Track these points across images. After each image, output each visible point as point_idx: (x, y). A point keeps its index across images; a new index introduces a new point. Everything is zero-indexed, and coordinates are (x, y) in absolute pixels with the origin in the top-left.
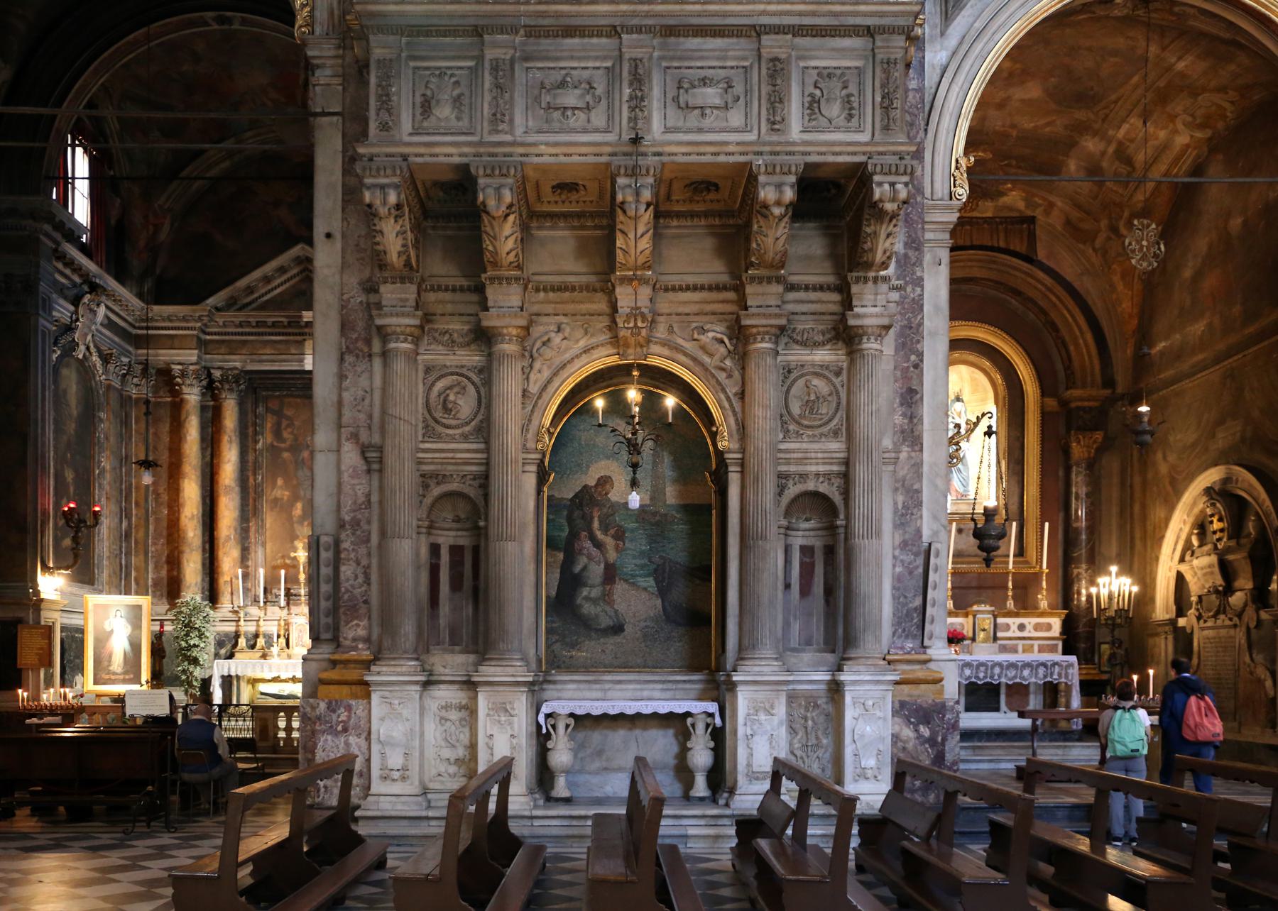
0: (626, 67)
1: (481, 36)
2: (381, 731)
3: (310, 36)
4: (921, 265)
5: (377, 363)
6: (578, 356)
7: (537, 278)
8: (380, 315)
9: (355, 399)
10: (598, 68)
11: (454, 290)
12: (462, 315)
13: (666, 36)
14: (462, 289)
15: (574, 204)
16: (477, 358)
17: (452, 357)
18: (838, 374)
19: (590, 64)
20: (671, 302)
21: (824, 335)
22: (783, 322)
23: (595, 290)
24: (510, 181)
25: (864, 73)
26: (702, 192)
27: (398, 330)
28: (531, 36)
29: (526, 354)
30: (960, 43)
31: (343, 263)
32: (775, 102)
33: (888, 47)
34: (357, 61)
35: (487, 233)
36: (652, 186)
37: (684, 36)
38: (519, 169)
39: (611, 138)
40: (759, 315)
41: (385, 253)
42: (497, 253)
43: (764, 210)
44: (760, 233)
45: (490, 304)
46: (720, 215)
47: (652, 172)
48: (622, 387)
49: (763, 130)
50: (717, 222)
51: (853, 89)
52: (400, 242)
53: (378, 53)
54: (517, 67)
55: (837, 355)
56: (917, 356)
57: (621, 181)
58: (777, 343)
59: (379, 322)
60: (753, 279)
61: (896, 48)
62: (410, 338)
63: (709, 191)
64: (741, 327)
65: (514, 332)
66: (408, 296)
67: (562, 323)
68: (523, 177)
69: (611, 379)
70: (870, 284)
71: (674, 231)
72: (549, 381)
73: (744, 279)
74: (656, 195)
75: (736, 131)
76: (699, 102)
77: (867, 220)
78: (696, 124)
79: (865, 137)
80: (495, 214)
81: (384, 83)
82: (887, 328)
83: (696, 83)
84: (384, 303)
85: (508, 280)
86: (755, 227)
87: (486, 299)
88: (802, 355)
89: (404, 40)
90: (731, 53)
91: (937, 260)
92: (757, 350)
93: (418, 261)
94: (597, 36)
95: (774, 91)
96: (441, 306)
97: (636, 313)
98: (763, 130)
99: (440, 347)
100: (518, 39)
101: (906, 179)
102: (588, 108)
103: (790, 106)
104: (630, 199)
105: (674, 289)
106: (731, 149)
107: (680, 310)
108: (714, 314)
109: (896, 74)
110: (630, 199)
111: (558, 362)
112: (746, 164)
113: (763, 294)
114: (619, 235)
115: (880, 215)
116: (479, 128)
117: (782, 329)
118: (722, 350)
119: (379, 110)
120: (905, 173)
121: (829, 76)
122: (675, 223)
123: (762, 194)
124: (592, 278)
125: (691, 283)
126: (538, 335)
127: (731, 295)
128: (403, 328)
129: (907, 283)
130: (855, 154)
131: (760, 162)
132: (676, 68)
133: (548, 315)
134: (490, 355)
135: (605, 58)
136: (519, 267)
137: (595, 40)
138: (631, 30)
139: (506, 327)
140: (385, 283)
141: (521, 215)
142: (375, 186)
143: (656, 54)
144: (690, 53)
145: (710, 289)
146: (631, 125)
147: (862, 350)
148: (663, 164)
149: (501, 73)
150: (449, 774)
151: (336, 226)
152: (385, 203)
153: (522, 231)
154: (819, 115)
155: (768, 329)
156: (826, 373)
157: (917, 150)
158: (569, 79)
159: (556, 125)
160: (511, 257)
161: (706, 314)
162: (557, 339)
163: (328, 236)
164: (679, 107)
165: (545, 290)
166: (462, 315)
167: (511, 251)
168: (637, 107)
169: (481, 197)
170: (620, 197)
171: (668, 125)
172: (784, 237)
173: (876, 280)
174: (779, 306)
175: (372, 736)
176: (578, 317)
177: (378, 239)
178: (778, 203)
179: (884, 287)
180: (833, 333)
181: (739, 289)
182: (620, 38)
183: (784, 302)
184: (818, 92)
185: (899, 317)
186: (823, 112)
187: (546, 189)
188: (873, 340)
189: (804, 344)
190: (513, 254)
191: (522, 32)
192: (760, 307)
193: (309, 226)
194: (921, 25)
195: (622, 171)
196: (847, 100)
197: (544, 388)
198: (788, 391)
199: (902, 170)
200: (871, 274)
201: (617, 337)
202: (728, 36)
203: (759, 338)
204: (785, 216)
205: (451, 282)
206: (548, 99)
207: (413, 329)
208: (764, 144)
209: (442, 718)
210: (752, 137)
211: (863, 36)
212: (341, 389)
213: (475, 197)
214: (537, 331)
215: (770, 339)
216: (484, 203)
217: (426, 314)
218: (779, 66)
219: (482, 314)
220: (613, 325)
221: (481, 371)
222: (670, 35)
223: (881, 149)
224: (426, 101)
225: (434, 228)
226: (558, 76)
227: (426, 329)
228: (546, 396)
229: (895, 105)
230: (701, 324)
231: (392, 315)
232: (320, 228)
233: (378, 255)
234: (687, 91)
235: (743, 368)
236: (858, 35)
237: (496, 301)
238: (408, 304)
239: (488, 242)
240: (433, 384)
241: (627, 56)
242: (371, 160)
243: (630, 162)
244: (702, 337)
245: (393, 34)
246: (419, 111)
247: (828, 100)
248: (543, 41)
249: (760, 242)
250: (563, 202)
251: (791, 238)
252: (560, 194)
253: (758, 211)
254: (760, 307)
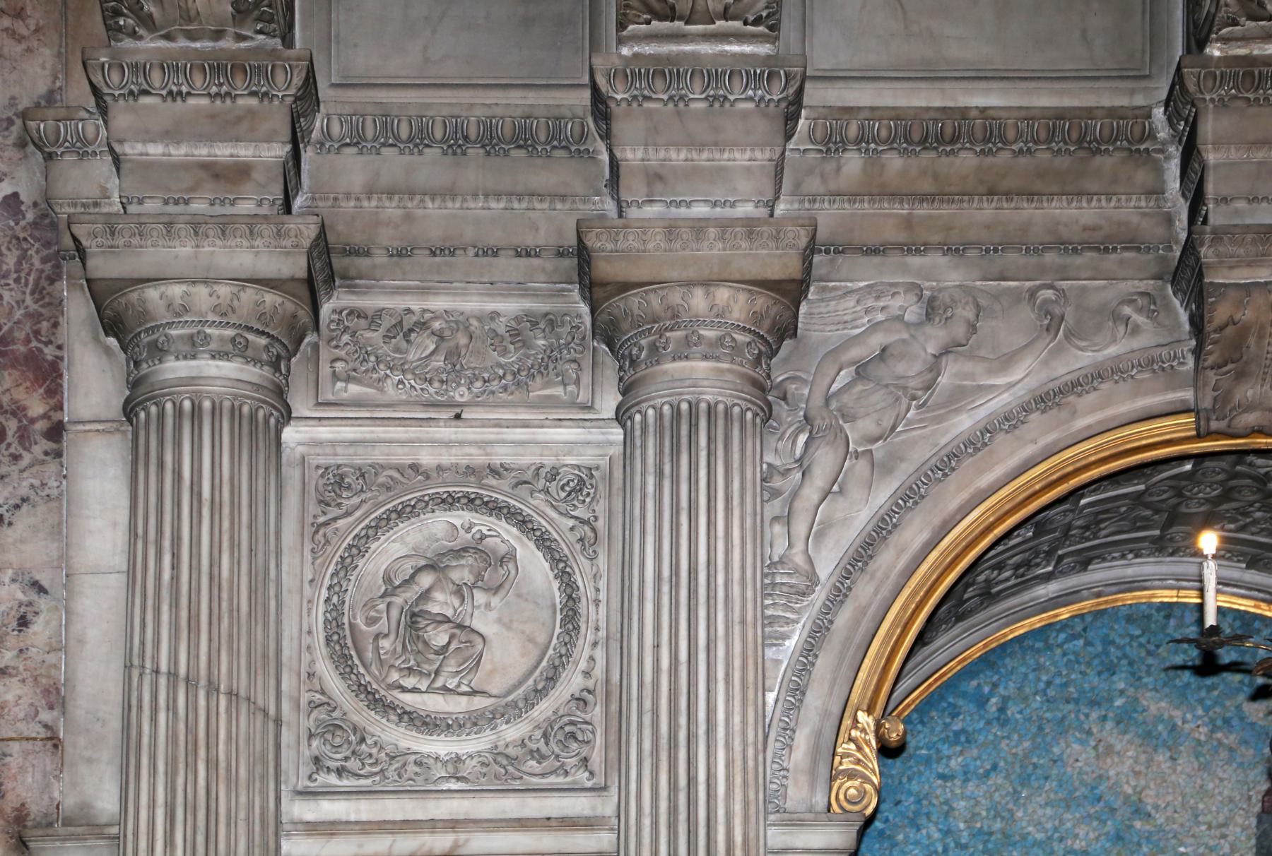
96: (391, 210)
240: (358, 548)
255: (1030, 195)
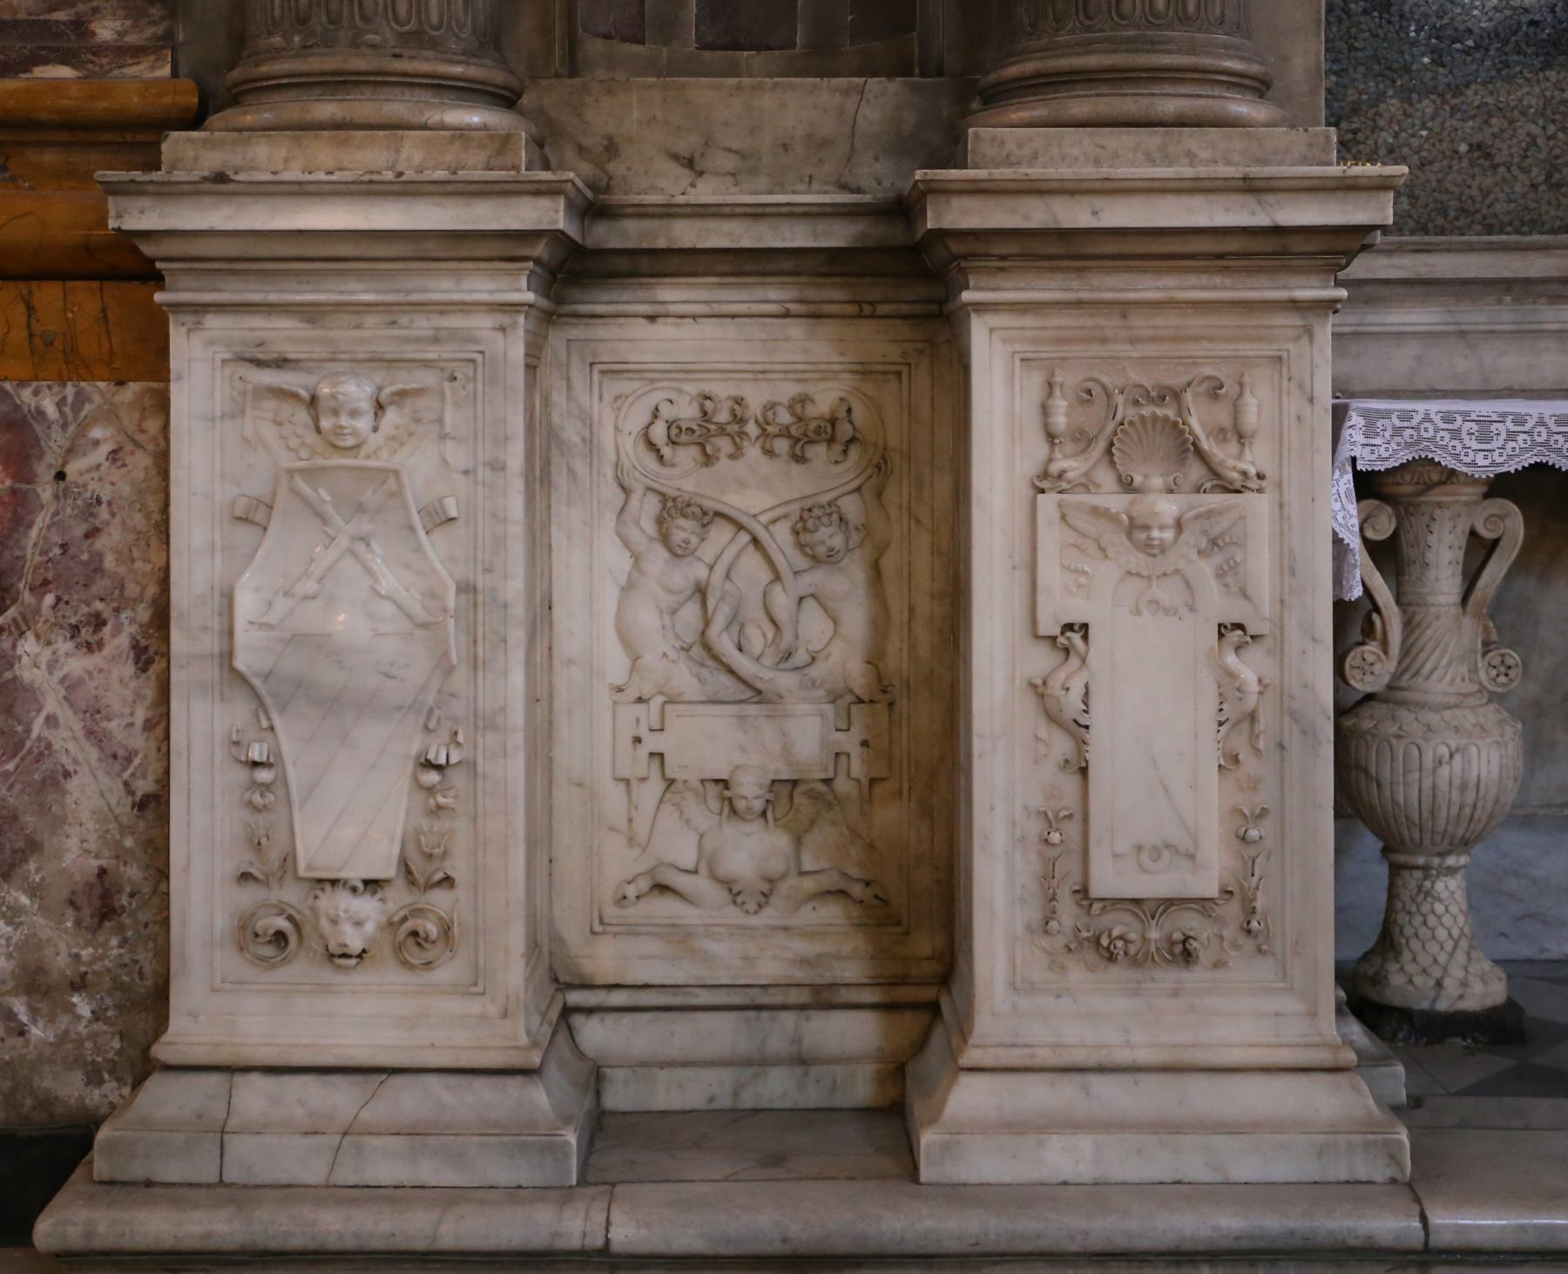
2: (246, 604)
150: (732, 890)
175: (179, 641)
209: (672, 507)
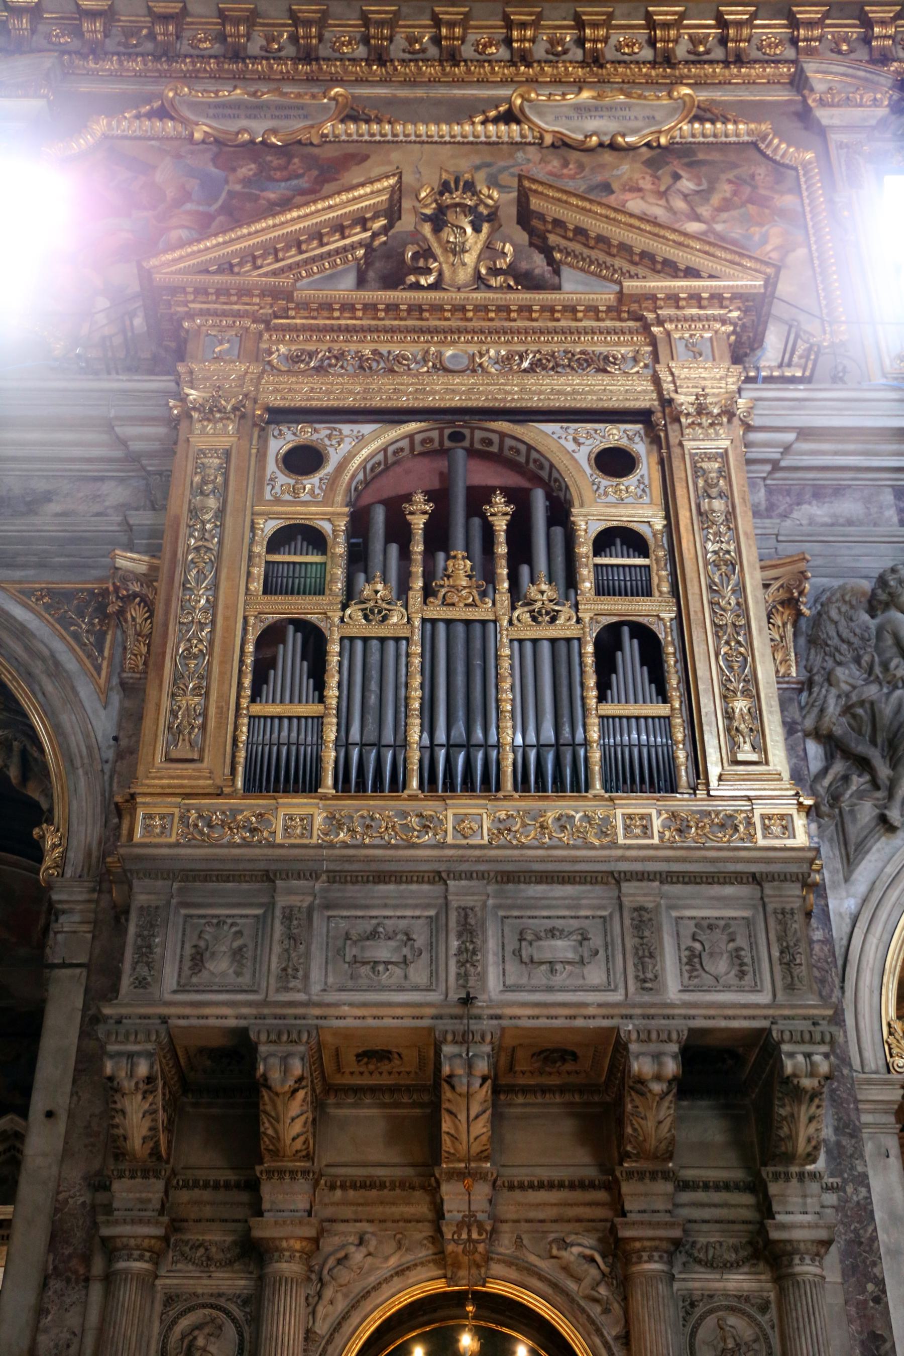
0: (453, 916)
1: (273, 882)
3: (59, 879)
4: (862, 1156)
5: (96, 1291)
6: (387, 1280)
7: (333, 1171)
8: (108, 1221)
9: (56, 1346)
10: (418, 917)
11: (216, 1186)
12: (226, 1221)
13: (502, 882)
14: (227, 1186)
15: (385, 1074)
16: (242, 1282)
17: (205, 1282)
18: (764, 1308)
19: (409, 913)
20: (519, 1204)
21: (736, 1251)
22: (677, 1233)
23: (413, 1188)
24: (302, 1048)
25: (754, 924)
26: (555, 1062)
27: (132, 1242)
28: (334, 882)
29: (313, 1276)
30: (871, 890)
31: (65, 1150)
32: (644, 957)
33: (781, 896)
34: (115, 906)
35: (265, 1112)
36: (489, 1056)
37: (525, 883)
38: (314, 1033)
39: (434, 997)
40: (642, 1223)
41: (125, 1138)
42: (279, 1139)
43: (639, 1086)
44: (636, 1114)
45: (266, 1206)
46: (581, 1089)
47: (488, 1038)
48: (452, 1323)
49: (632, 989)
50: (577, 1098)
51: (741, 941)
52: (147, 1123)
53: (141, 899)
54: (316, 916)
55: (760, 1281)
56: (876, 1285)
57: (448, 1049)
58: (670, 1263)
59: (105, 1231)
60: (630, 1174)
61: (793, 896)
62: (148, 1254)
63: (564, 1061)
64: (619, 1242)
65: (298, 1245)
66: (150, 1195)
67: (365, 1233)
68: (319, 1043)
69: (435, 1311)
70: (794, 1181)
71: (519, 1110)
72: (345, 1317)
73: (618, 1174)
74: (495, 1066)
75: (595, 989)
76: (548, 956)
77: (780, 1099)
78: (544, 981)
79: (764, 998)
80: (279, 1089)
81: (146, 933)
82: (827, 1244)
83: (543, 934)
84: (115, 1205)
85: (293, 1173)
86: (629, 1107)
87: (259, 1200)
88: (707, 1280)
89: (176, 885)
90: (584, 902)
91: (883, 1150)
92: (642, 1273)
93: (169, 1147)
94: (417, 882)
95: (642, 945)
97: (468, 1221)
98: (632, 989)
99: (191, 1267)
100: (318, 886)
101: (825, 1049)
102: (405, 962)
103: (663, 961)
104: (460, 1071)
105: (522, 1187)
106: (591, 1011)
107: (532, 1214)
108: (579, 1220)
109: (794, 926)
110: (460, 1071)
111: (357, 1288)
112: (611, 1029)
113: (646, 1195)
114: (446, 1118)
115: (797, 1094)
116: (264, 985)
117: (677, 1243)
118: (594, 1272)
119: (137, 963)
120: (823, 1042)
121: (710, 927)
122: (520, 1099)
123: (635, 1067)
124: (409, 1171)
125: (545, 1179)
126: (331, 1249)
127: (602, 1195)
128: (139, 1241)
129: (845, 1181)
130: (753, 1018)
131: (630, 1027)
132: (516, 917)
133: (347, 1221)
134: (261, 1278)
135: (427, 906)
136: (309, 1157)
137: (414, 887)
138: (458, 876)
139: (287, 1239)
140: (120, 1177)
141: (313, 1090)
142: (119, 1054)
143: (491, 902)
144: (533, 901)
145: (572, 1186)
146: (461, 982)
147: (794, 1275)
148: (503, 1029)
149: (295, 922)
151: (62, 1101)
152: (131, 1075)
153: (315, 1109)
154: (701, 971)
155: (657, 1243)
156: (749, 1309)
157: (835, 1013)
158: (381, 929)
159: (363, 982)
160: (299, 1144)
161: (569, 1221)
162: (358, 1256)
163: (50, 1114)
164: (522, 962)
165: (343, 1187)
166: (226, 1221)
167: (298, 1135)
168: (467, 961)
169: (261, 1068)
170: (446, 1070)
171: (508, 983)
172: (669, 1120)
173: (801, 1176)
174: (669, 1211)
176: (389, 1224)
177: (117, 1120)
178: (658, 1078)
179: (814, 1187)
180: (750, 1250)
181: (612, 1186)
182: (446, 884)
183: (676, 1205)
184: (697, 946)
185: (841, 1228)
186: (707, 968)
187: (349, 1057)
188: (808, 1261)
189: (710, 1265)
190: (301, 1139)
191: (324, 877)
192: (644, 1211)
193: (26, 1091)
194: (818, 871)
195: (450, 1037)
196: (736, 956)
197: (337, 1327)
198: (693, 1334)
199: (818, 1037)
200: (794, 1169)
201: (442, 1252)
202: (580, 883)
203: (645, 1256)
204: (667, 1094)
205: (213, 1176)
206: (354, 951)
207: (153, 1241)
208: (634, 1006)
210: (618, 997)
211: (748, 883)
212: (36, 1330)
213: (254, 1067)
214: (329, 1244)
215: (661, 1257)
216: (265, 1076)
217: (173, 1220)
218: (646, 916)
219: (253, 1221)
220: (437, 1237)
221: (246, 1302)
222: (508, 882)
223: (787, 1012)
224: (198, 953)
225: (195, 1105)
226: (368, 926)
227: (172, 1240)
228: (339, 1340)
229: (798, 961)
230: (562, 1235)
231: (125, 1222)
232: (39, 1103)
233: (114, 1141)
234: (531, 944)
235: (625, 1299)
236: (741, 883)
237: (273, 1203)
238: (151, 1206)
239: (267, 1125)
240: (174, 1322)
241: (454, 904)
242: (119, 1022)
243: (459, 1026)
244: (564, 1254)
245: (164, 879)
246: (187, 964)
247: (711, 955)
248: (350, 887)
249: (636, 1126)
250: (371, 1073)
251: (679, 1120)
252: (367, 1064)
253: (632, 1088)
254: (644, 1211)
255: (394, 1204)
